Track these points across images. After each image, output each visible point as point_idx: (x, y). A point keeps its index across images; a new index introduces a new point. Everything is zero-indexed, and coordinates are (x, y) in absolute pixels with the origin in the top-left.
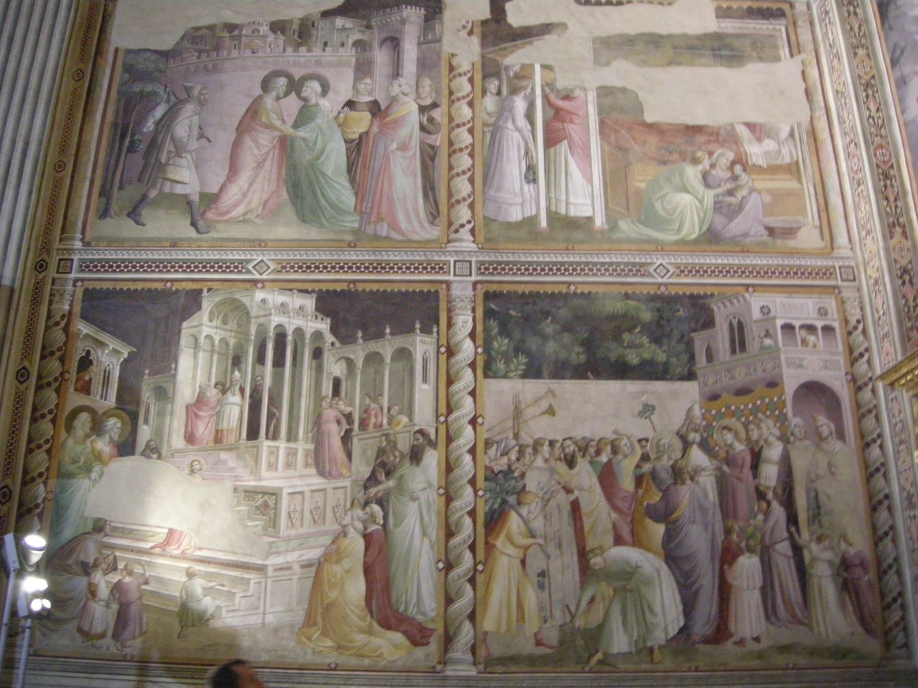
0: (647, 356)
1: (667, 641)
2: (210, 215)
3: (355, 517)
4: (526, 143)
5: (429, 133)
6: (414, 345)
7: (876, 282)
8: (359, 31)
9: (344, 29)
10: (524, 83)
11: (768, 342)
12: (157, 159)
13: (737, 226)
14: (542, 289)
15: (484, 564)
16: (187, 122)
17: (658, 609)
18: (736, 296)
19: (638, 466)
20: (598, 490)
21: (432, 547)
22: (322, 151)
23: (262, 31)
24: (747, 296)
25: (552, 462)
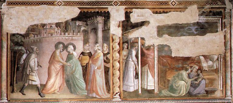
2: (44, 91)
4: (136, 66)
5: (107, 63)
8: (84, 26)
9: (79, 26)
12: (26, 73)
13: (196, 91)
16: (33, 60)
23: (53, 27)
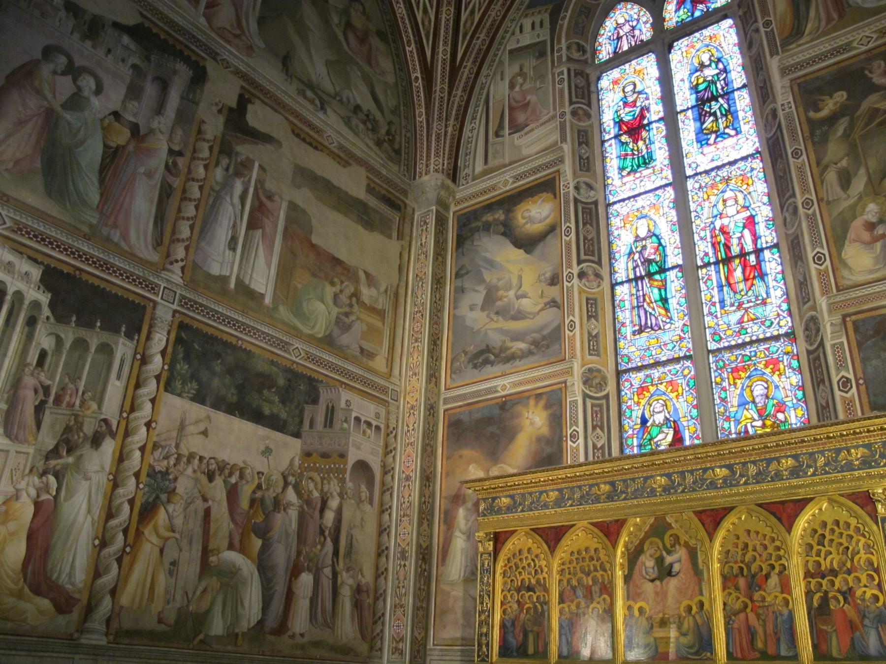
0: (275, 411)
1: (249, 629)
3: (31, 483)
5: (171, 173)
6: (117, 344)
7: (413, 407)
9: (126, 48)
10: (246, 172)
11: (345, 425)
13: (345, 339)
14: (220, 336)
15: (131, 548)
17: (246, 605)
18: (334, 386)
19: (254, 492)
20: (225, 503)
21: (93, 525)
22: (82, 143)
24: (340, 389)
25: (199, 474)
